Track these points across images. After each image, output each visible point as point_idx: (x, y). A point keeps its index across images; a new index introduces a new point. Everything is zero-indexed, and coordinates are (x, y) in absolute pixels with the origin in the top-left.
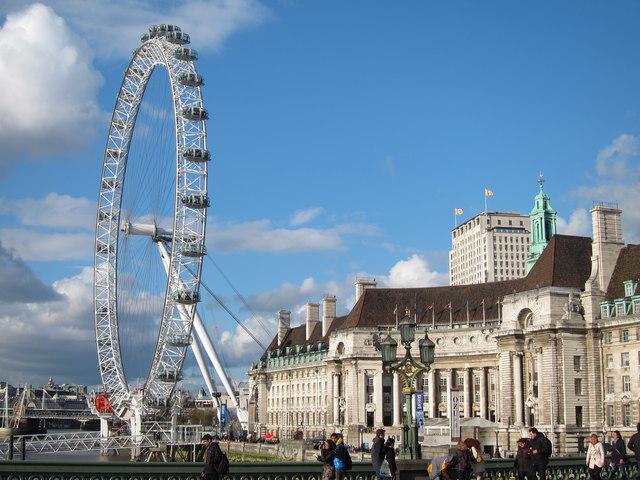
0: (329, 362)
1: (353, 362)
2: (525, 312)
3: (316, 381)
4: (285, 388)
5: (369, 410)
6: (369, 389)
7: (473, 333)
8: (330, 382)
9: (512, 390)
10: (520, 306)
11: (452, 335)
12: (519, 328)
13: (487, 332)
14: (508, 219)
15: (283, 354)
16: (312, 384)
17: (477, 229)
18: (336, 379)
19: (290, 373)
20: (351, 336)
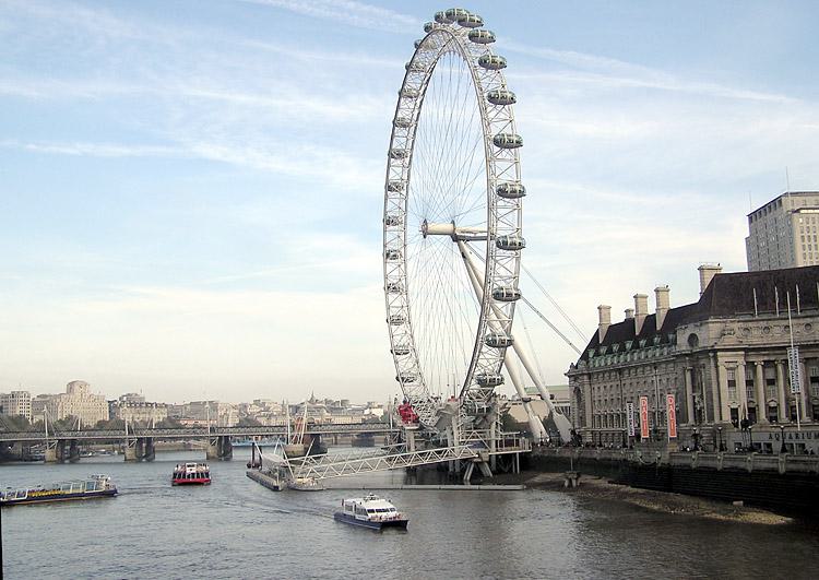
1: (711, 354)
6: (732, 384)
15: (610, 351)
18: (688, 375)
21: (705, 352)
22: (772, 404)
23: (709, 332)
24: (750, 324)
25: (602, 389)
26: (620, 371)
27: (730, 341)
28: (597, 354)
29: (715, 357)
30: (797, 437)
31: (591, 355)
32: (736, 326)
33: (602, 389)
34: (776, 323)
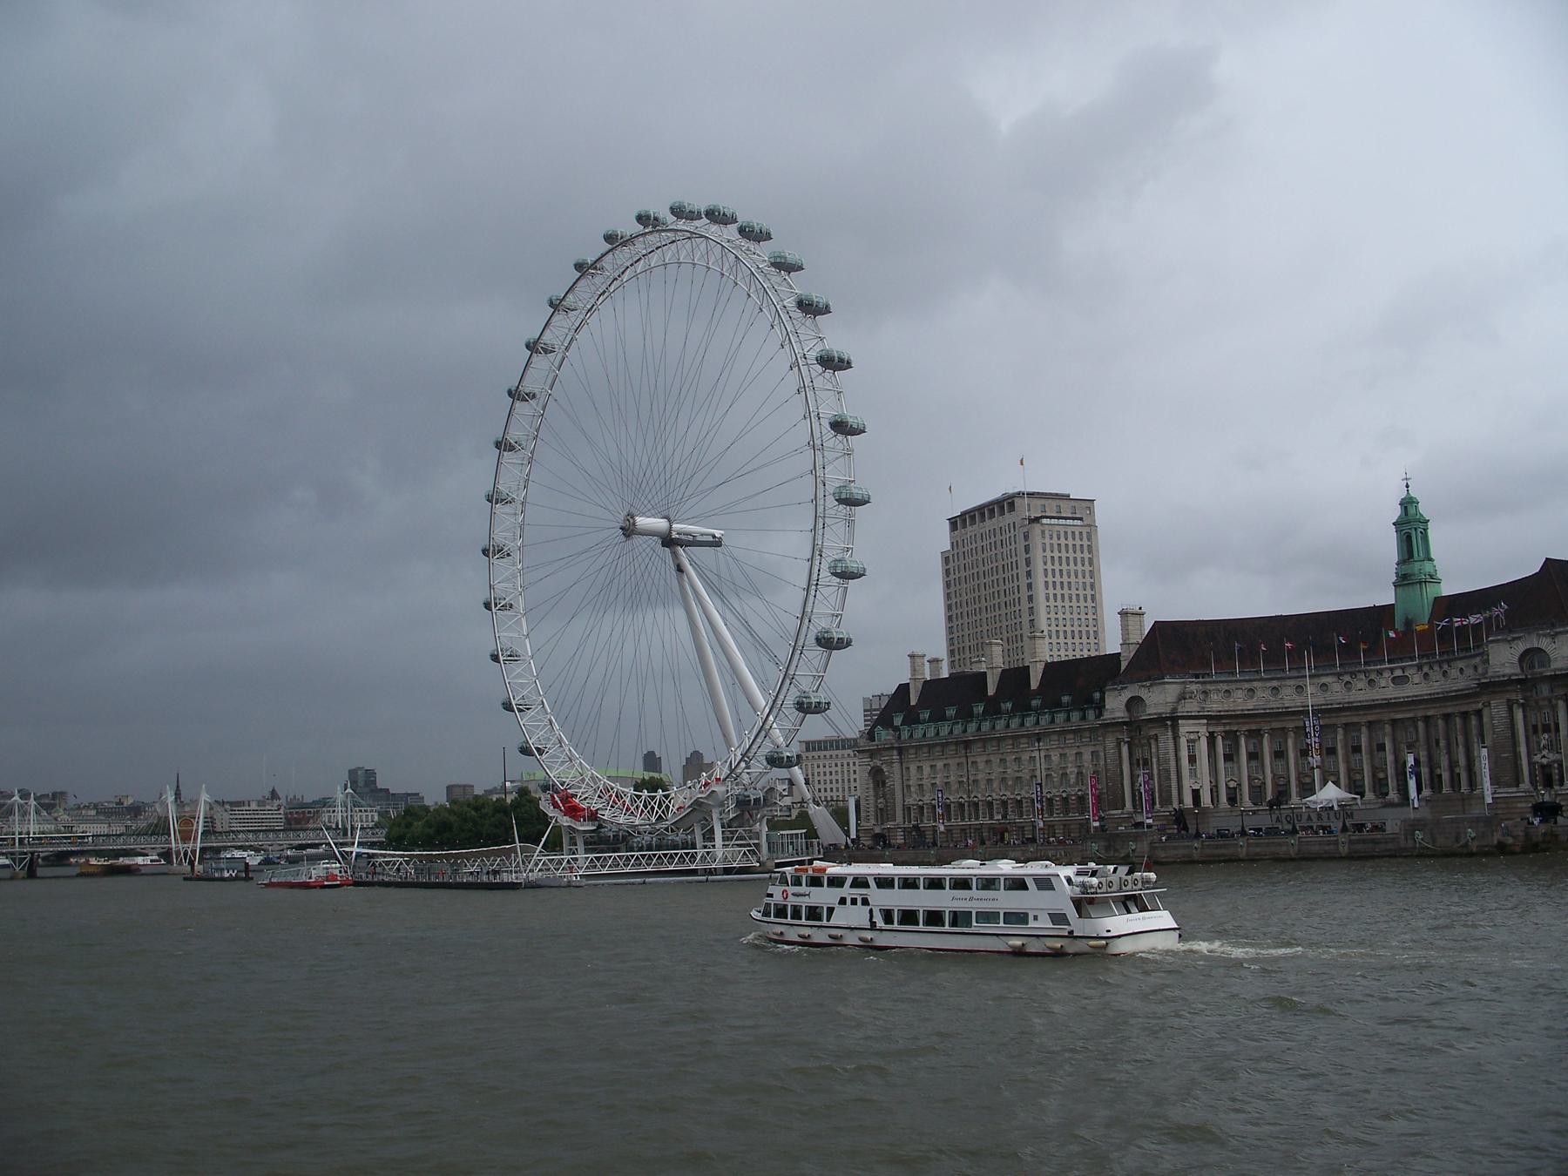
0: (1106, 726)
2: (1527, 652)
3: (1036, 754)
4: (953, 768)
5: (1196, 787)
6: (1192, 759)
7: (1324, 680)
8: (1111, 751)
9: (1515, 744)
10: (1521, 647)
11: (1291, 682)
12: (1518, 670)
13: (1347, 678)
14: (1054, 503)
16: (1025, 757)
17: (1009, 518)
18: (1125, 749)
19: (967, 744)
20: (1155, 688)
21: (1160, 721)
22: (1232, 784)
23: (1159, 698)
24: (1208, 687)
25: (927, 770)
26: (967, 744)
27: (1191, 707)
28: (912, 719)
29: (1175, 728)
30: (1319, 817)
31: (898, 721)
32: (1194, 687)
33: (927, 770)
34: (1239, 685)
